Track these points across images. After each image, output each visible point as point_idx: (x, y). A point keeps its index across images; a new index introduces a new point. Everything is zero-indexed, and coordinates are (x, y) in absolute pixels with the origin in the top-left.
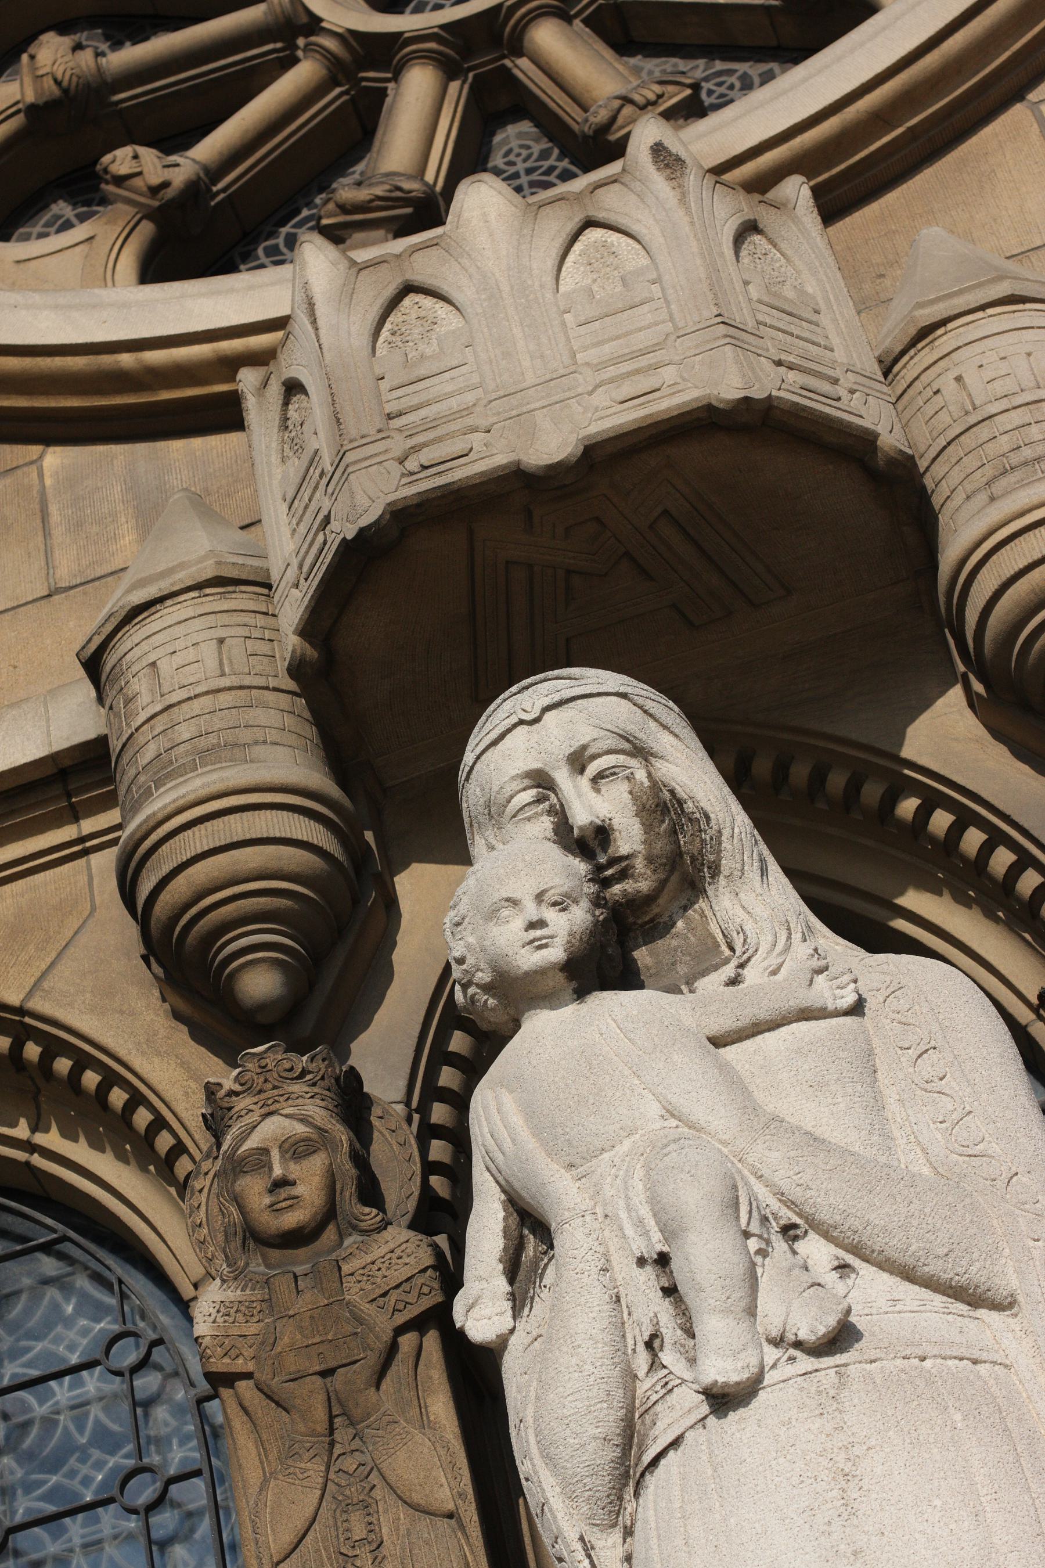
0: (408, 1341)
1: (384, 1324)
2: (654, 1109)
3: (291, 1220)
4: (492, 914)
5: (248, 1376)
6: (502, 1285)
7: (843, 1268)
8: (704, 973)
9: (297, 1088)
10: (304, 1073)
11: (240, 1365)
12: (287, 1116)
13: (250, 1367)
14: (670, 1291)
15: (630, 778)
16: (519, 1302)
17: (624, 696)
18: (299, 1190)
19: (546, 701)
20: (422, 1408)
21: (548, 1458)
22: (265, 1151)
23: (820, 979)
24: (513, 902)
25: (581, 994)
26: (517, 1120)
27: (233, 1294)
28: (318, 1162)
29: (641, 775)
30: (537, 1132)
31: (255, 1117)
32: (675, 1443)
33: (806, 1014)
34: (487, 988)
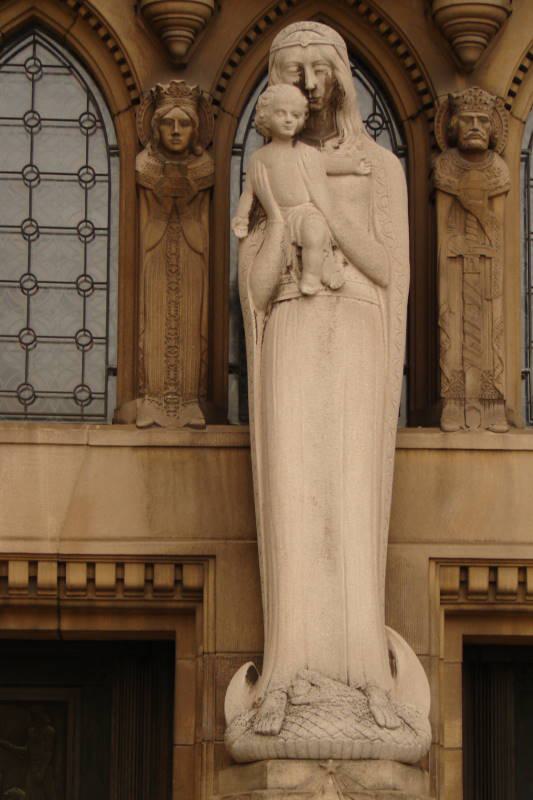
0: (200, 196)
1: (195, 187)
2: (308, 199)
3: (177, 147)
4: (277, 111)
5: (151, 190)
6: (247, 221)
7: (345, 264)
8: (328, 139)
9: (187, 100)
10: (191, 94)
11: (149, 186)
12: (183, 110)
13: (152, 187)
14: (300, 257)
15: (327, 74)
16: (251, 228)
17: (333, 45)
18: (181, 138)
19: (310, 41)
20: (200, 216)
21: (252, 288)
22: (173, 121)
23: (362, 164)
24: (284, 112)
25: (294, 144)
26: (266, 179)
27: (152, 161)
28: (189, 129)
29: (330, 73)
30: (272, 187)
31: (171, 106)
32: (289, 300)
33: (355, 174)
34: (268, 129)
